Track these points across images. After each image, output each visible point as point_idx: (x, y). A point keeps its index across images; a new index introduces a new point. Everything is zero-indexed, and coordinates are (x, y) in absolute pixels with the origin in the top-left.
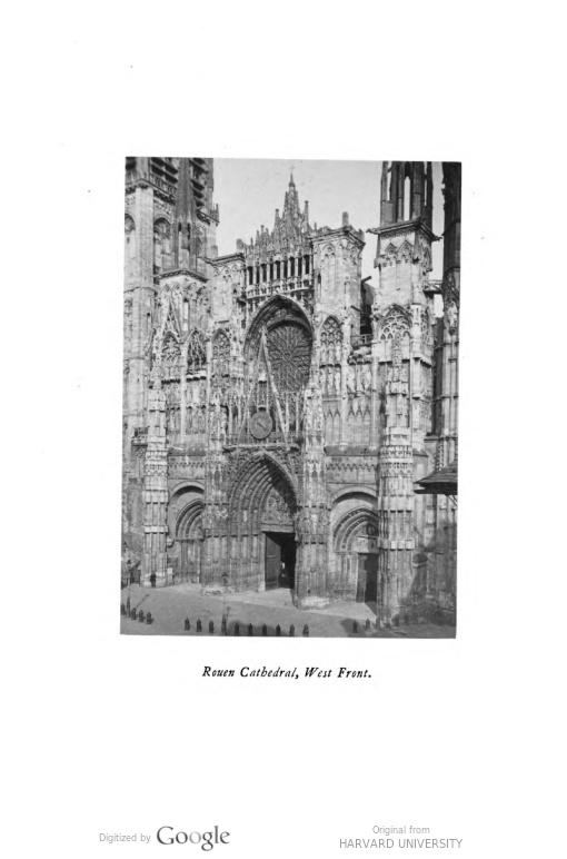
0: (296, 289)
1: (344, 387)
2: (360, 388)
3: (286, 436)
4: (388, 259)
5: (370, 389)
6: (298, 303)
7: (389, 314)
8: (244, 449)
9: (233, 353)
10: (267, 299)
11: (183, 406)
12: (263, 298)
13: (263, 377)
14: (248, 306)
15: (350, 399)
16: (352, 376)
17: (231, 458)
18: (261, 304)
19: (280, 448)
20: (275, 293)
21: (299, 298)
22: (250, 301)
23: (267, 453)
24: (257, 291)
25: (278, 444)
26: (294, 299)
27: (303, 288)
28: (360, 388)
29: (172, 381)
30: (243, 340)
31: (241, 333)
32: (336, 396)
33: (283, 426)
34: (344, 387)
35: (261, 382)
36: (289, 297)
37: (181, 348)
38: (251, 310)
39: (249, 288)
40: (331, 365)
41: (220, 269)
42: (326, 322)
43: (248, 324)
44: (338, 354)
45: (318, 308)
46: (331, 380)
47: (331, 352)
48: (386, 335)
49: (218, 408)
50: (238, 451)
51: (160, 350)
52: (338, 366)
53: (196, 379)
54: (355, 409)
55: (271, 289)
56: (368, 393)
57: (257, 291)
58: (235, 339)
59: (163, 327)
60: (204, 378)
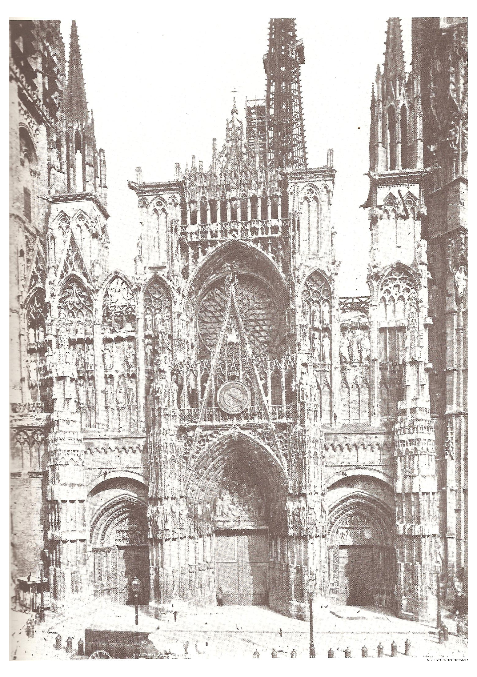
0: (260, 235)
1: (336, 354)
2: (356, 356)
3: (270, 411)
4: (386, 211)
5: (368, 359)
6: (265, 253)
7: (390, 274)
8: (206, 428)
9: (176, 308)
10: (219, 245)
11: (100, 375)
12: (213, 243)
13: (233, 338)
14: (191, 251)
15: (343, 369)
16: (347, 343)
17: (189, 441)
18: (210, 250)
19: (260, 426)
20: (230, 237)
21: (265, 248)
22: (194, 245)
23: (242, 432)
24: (204, 233)
25: (257, 421)
26: (259, 247)
27: (270, 234)
28: (356, 356)
29: (80, 341)
30: (186, 293)
31: (184, 285)
32: (324, 365)
33: (264, 398)
34: (336, 354)
35: (231, 343)
36: (250, 244)
37: (94, 296)
38: (196, 257)
39: (192, 228)
40: (317, 329)
41: (150, 199)
42: (310, 278)
43: (192, 275)
44: (326, 316)
45: (297, 260)
46: (318, 347)
47: (317, 314)
48: (387, 297)
49: (168, 374)
50: (199, 430)
51: (58, 298)
52: (327, 330)
53: (119, 340)
54: (350, 381)
55: (224, 232)
56: (367, 363)
57: (204, 233)
58: (178, 290)
59: (61, 268)
60: (131, 339)
